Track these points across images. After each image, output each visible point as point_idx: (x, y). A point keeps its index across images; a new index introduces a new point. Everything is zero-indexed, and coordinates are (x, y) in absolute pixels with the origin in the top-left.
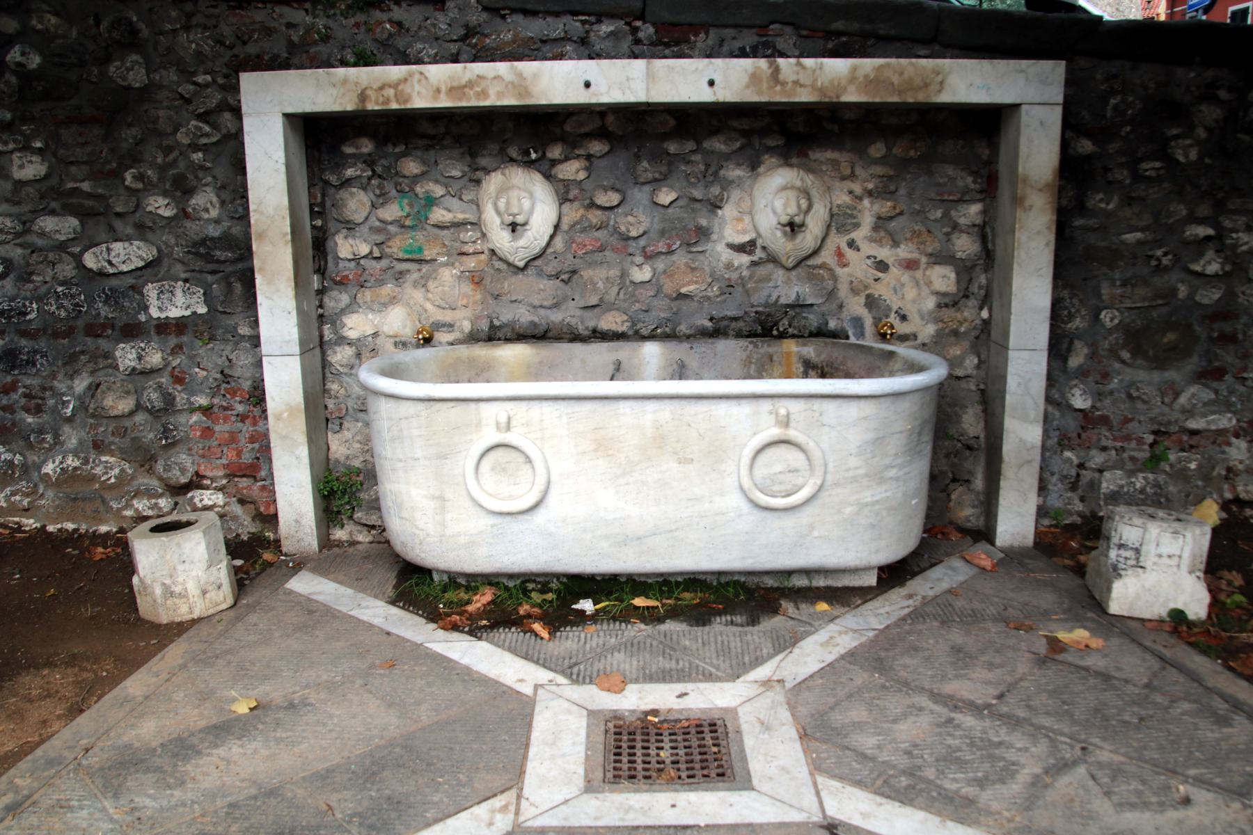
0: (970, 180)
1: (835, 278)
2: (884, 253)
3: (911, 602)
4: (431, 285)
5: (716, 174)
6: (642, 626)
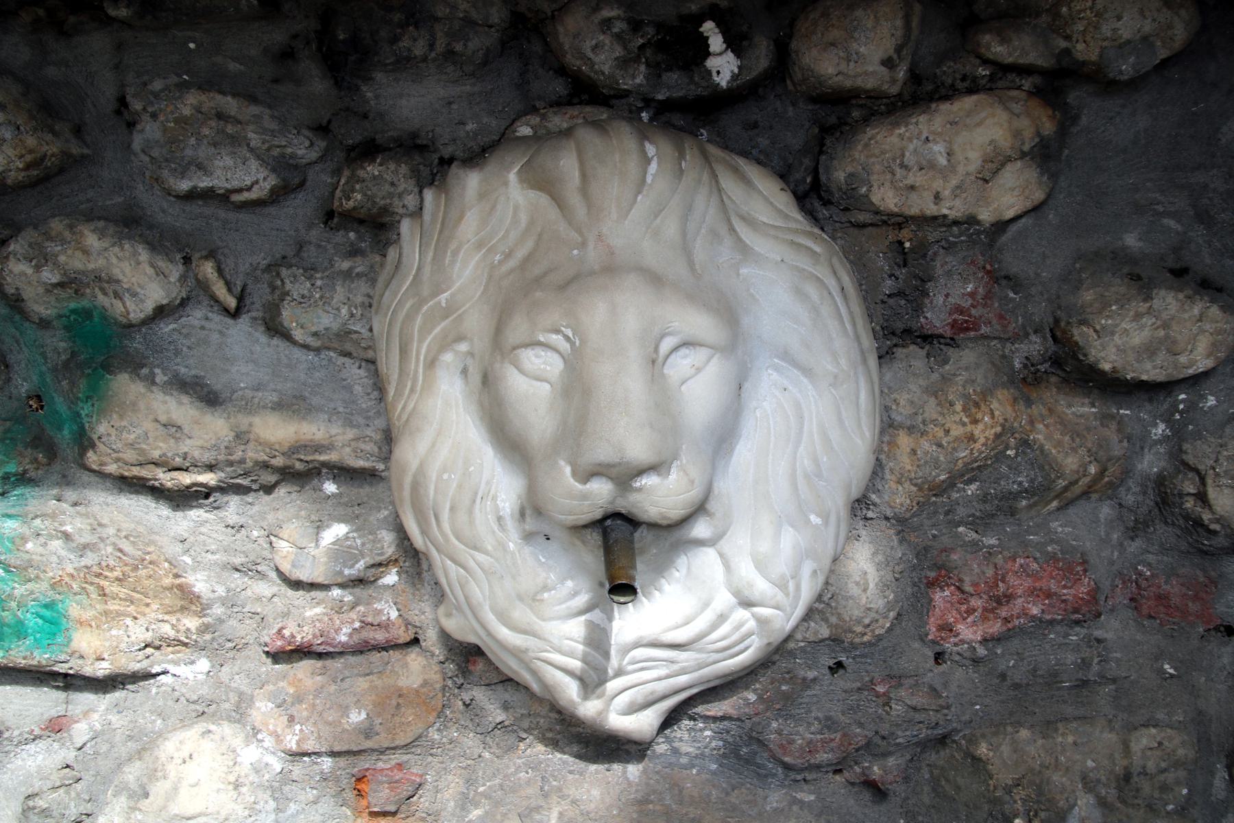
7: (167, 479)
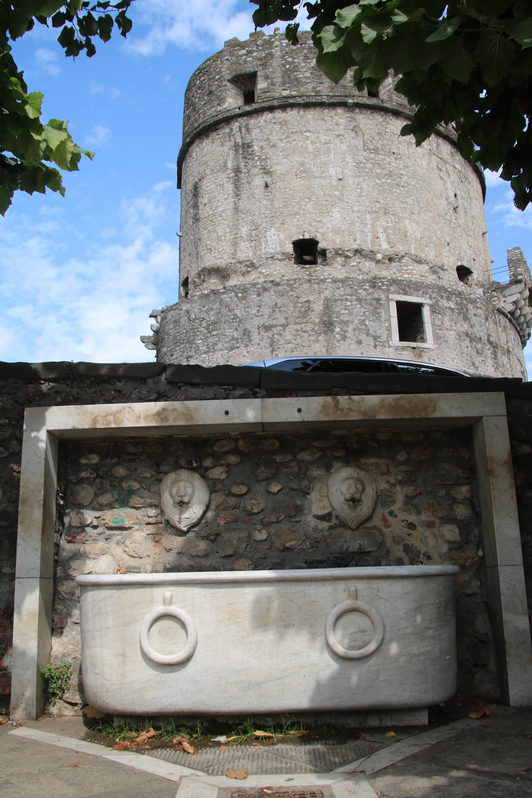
0: (459, 471)
1: (383, 535)
2: (412, 518)
3: (454, 731)
4: (128, 542)
5: (305, 474)
6: (261, 747)
7: (137, 506)
